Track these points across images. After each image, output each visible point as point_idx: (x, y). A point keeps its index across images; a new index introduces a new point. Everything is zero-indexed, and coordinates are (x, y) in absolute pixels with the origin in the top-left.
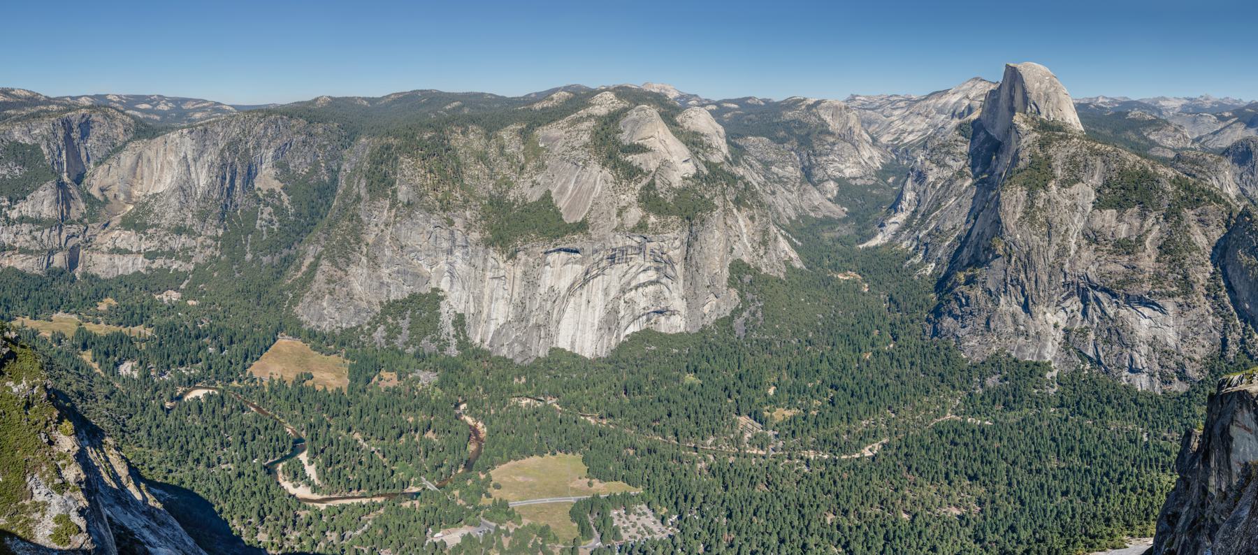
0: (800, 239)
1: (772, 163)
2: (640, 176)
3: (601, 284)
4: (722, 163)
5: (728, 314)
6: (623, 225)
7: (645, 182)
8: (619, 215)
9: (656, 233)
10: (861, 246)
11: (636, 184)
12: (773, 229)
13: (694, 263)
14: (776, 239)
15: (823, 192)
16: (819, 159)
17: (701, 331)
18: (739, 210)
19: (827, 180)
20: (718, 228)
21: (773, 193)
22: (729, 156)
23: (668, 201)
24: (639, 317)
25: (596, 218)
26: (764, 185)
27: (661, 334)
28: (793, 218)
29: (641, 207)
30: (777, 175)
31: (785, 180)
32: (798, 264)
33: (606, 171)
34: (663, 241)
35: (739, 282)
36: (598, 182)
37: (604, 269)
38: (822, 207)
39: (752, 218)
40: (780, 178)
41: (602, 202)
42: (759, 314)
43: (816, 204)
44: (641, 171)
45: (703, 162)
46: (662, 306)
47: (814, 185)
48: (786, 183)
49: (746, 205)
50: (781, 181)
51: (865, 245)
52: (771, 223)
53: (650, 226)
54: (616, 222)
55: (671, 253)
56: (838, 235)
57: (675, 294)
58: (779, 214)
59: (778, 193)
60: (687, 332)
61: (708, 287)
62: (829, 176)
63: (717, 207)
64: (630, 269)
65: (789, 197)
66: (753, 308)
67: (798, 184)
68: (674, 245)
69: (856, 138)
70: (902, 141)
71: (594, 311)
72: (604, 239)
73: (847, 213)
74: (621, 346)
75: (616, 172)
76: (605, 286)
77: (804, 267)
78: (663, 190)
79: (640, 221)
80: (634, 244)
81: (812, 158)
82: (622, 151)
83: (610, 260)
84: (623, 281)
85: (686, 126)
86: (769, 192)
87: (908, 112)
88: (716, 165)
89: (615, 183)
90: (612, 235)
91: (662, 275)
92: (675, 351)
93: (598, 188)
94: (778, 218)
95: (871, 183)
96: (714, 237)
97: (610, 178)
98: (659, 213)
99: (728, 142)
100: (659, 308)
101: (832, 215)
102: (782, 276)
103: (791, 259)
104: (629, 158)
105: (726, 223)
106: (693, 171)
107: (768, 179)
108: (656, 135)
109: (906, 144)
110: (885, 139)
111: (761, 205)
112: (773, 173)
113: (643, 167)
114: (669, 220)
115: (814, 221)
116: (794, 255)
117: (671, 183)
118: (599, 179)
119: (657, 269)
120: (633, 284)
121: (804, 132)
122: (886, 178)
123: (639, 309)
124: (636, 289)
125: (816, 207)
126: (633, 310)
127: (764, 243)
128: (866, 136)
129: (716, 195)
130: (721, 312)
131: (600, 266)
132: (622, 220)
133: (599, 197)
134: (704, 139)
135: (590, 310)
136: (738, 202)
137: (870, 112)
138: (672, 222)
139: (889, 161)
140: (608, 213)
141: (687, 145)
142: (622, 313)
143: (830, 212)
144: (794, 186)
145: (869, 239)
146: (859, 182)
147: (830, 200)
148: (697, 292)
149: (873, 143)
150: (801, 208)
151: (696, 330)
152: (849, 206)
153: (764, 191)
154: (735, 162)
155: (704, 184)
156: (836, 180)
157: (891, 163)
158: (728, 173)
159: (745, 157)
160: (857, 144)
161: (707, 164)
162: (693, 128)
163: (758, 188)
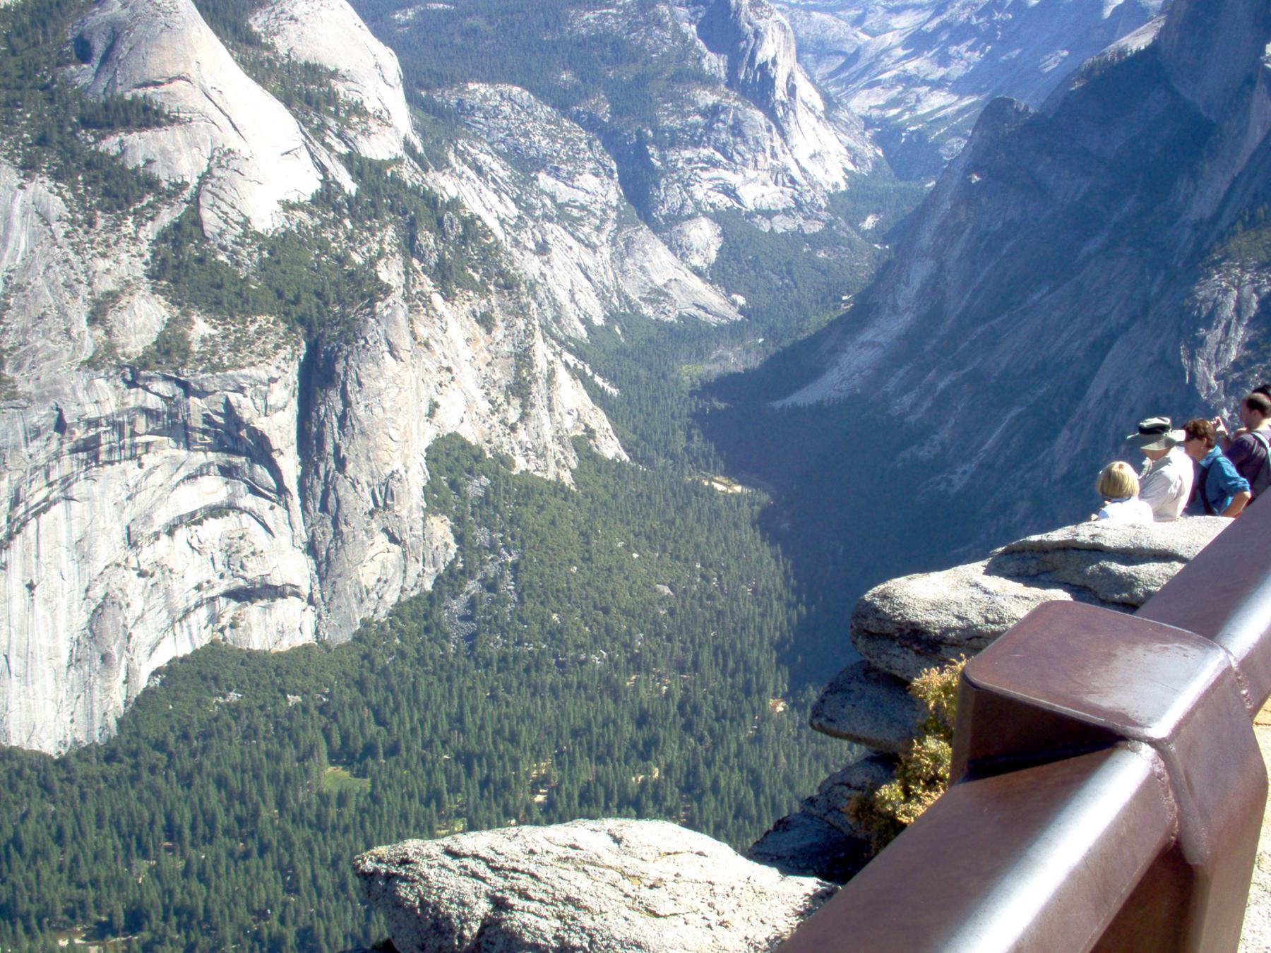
0: (613, 379)
1: (540, 163)
2: (149, 198)
3: (63, 527)
4: (398, 161)
5: (428, 586)
6: (111, 348)
7: (167, 216)
8: (96, 317)
9: (214, 368)
10: (777, 405)
11: (139, 225)
12: (542, 351)
13: (329, 448)
14: (551, 375)
15: (680, 250)
16: (672, 155)
17: (358, 637)
18: (448, 297)
19: (690, 217)
20: (392, 350)
21: (542, 249)
22: (416, 141)
23: (242, 274)
24: (187, 612)
25: (25, 331)
26: (516, 227)
27: (251, 654)
28: (598, 321)
29: (162, 292)
30: (553, 198)
31: (575, 213)
32: (611, 448)
33: (41, 187)
34: (240, 390)
35: (453, 497)
36: (16, 222)
37: (67, 481)
38: (674, 292)
39: (485, 321)
40: (560, 207)
41: (40, 281)
42: (508, 585)
43: (659, 281)
44: (151, 184)
45: (340, 157)
46: (249, 575)
47: (656, 229)
48: (576, 221)
49: (468, 284)
50: (564, 215)
51: (788, 402)
52: (538, 334)
53: (195, 348)
54: (89, 339)
55: (261, 424)
56: (716, 369)
57: (284, 537)
58: (557, 307)
59: (557, 254)
60: (321, 642)
61: (371, 513)
62: (697, 204)
63: (387, 290)
64: (147, 476)
65: (588, 260)
66: (491, 569)
67: (610, 226)
68: (271, 400)
69: (780, 95)
70: (912, 109)
71: (53, 611)
72: (57, 393)
73: (742, 311)
74: (142, 704)
75: (73, 189)
76: (77, 535)
77: (625, 457)
78: (228, 240)
79: (161, 335)
80: (153, 402)
81: (652, 150)
82: (86, 123)
83: (82, 455)
84: (130, 511)
85: (281, 45)
86: (531, 245)
87: (936, 21)
88: (378, 167)
89: (72, 222)
90: (81, 380)
91: (243, 485)
92: (293, 699)
93: (20, 239)
94: (557, 319)
95: (814, 227)
96: (382, 374)
97: (57, 206)
98: (215, 308)
99: (411, 99)
100: (241, 583)
101: (701, 314)
102: (567, 478)
103: (590, 433)
104: (110, 145)
105: (414, 336)
106: (310, 184)
107: (529, 209)
108: (193, 72)
109: (922, 119)
110: (863, 102)
111: (509, 285)
112: (542, 192)
113: (161, 173)
114: (252, 328)
115: (653, 331)
116: (600, 421)
117: (248, 220)
118: (17, 210)
119: (228, 472)
120: (162, 518)
121: (628, 73)
122: (854, 219)
123: (183, 595)
124: (171, 533)
125: (659, 292)
126: (168, 594)
127: (520, 389)
128: (806, 91)
129: (381, 254)
130: (410, 582)
131: (55, 475)
132: (108, 333)
133: (27, 267)
134: (339, 87)
135: (40, 609)
136: (445, 276)
137: (826, 17)
138: (259, 333)
139: (869, 167)
140: (63, 314)
141: (288, 103)
142: (137, 606)
143: (699, 307)
144: (598, 229)
145: (799, 387)
146: (782, 225)
147: (697, 272)
148: (344, 528)
149: (826, 112)
150: (621, 294)
151: (344, 637)
152: (750, 293)
153: (517, 243)
154: (433, 159)
155: (347, 222)
156: (718, 217)
157: (873, 175)
158: (415, 191)
159: (462, 144)
160: (780, 112)
161: (352, 162)
162: (305, 53)
163: (500, 234)
